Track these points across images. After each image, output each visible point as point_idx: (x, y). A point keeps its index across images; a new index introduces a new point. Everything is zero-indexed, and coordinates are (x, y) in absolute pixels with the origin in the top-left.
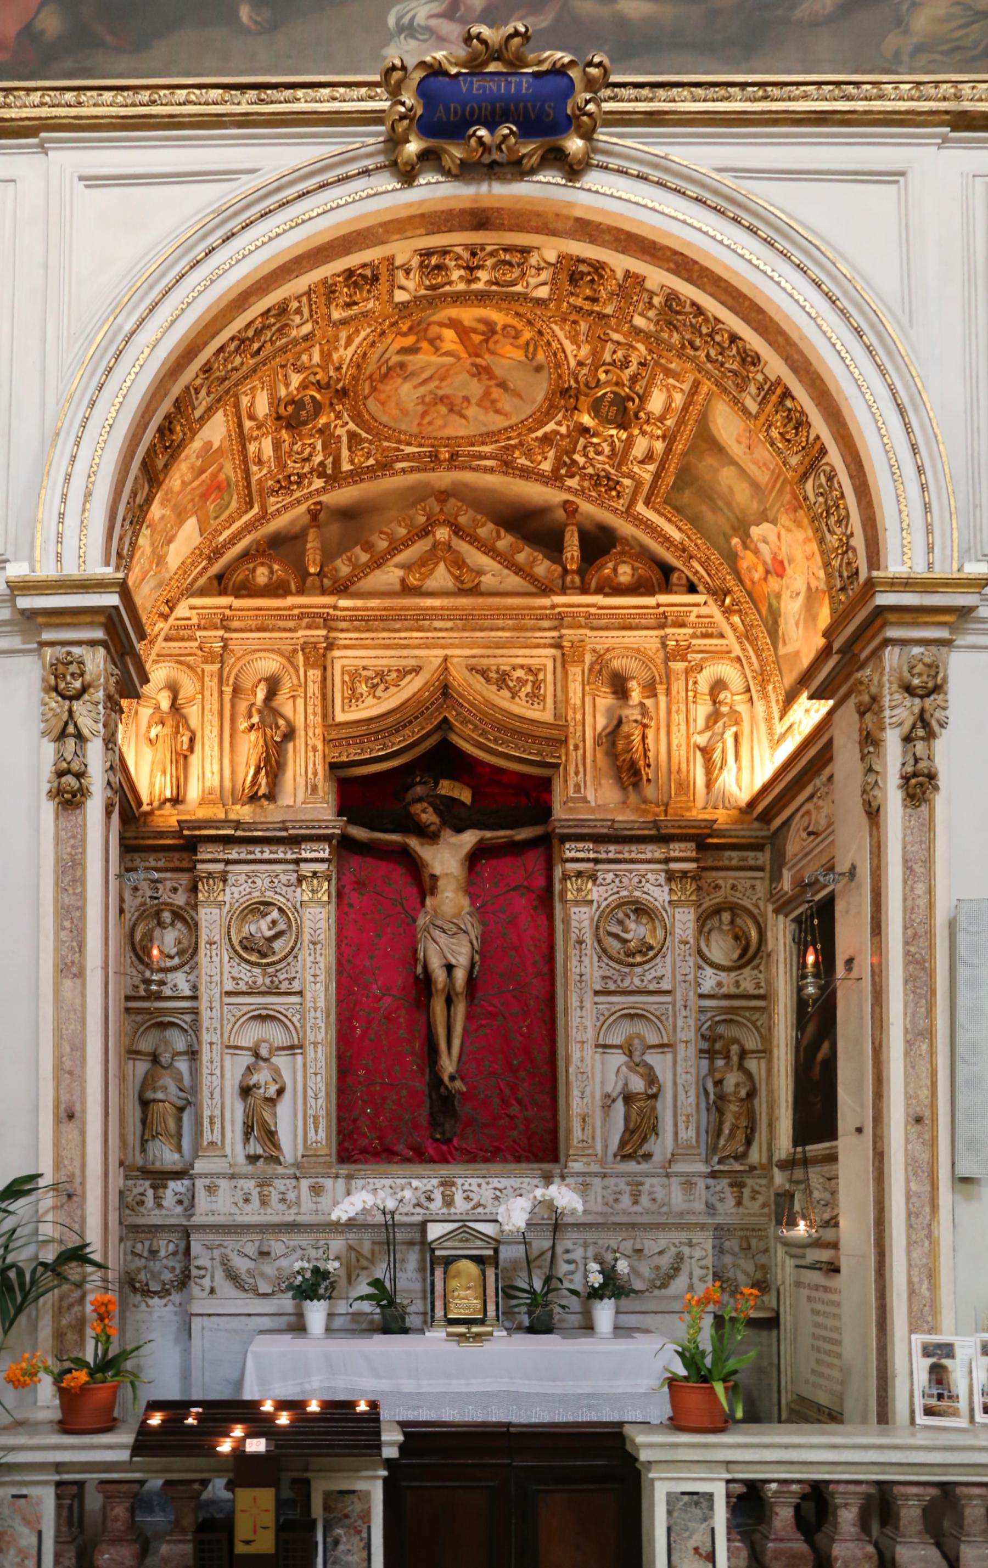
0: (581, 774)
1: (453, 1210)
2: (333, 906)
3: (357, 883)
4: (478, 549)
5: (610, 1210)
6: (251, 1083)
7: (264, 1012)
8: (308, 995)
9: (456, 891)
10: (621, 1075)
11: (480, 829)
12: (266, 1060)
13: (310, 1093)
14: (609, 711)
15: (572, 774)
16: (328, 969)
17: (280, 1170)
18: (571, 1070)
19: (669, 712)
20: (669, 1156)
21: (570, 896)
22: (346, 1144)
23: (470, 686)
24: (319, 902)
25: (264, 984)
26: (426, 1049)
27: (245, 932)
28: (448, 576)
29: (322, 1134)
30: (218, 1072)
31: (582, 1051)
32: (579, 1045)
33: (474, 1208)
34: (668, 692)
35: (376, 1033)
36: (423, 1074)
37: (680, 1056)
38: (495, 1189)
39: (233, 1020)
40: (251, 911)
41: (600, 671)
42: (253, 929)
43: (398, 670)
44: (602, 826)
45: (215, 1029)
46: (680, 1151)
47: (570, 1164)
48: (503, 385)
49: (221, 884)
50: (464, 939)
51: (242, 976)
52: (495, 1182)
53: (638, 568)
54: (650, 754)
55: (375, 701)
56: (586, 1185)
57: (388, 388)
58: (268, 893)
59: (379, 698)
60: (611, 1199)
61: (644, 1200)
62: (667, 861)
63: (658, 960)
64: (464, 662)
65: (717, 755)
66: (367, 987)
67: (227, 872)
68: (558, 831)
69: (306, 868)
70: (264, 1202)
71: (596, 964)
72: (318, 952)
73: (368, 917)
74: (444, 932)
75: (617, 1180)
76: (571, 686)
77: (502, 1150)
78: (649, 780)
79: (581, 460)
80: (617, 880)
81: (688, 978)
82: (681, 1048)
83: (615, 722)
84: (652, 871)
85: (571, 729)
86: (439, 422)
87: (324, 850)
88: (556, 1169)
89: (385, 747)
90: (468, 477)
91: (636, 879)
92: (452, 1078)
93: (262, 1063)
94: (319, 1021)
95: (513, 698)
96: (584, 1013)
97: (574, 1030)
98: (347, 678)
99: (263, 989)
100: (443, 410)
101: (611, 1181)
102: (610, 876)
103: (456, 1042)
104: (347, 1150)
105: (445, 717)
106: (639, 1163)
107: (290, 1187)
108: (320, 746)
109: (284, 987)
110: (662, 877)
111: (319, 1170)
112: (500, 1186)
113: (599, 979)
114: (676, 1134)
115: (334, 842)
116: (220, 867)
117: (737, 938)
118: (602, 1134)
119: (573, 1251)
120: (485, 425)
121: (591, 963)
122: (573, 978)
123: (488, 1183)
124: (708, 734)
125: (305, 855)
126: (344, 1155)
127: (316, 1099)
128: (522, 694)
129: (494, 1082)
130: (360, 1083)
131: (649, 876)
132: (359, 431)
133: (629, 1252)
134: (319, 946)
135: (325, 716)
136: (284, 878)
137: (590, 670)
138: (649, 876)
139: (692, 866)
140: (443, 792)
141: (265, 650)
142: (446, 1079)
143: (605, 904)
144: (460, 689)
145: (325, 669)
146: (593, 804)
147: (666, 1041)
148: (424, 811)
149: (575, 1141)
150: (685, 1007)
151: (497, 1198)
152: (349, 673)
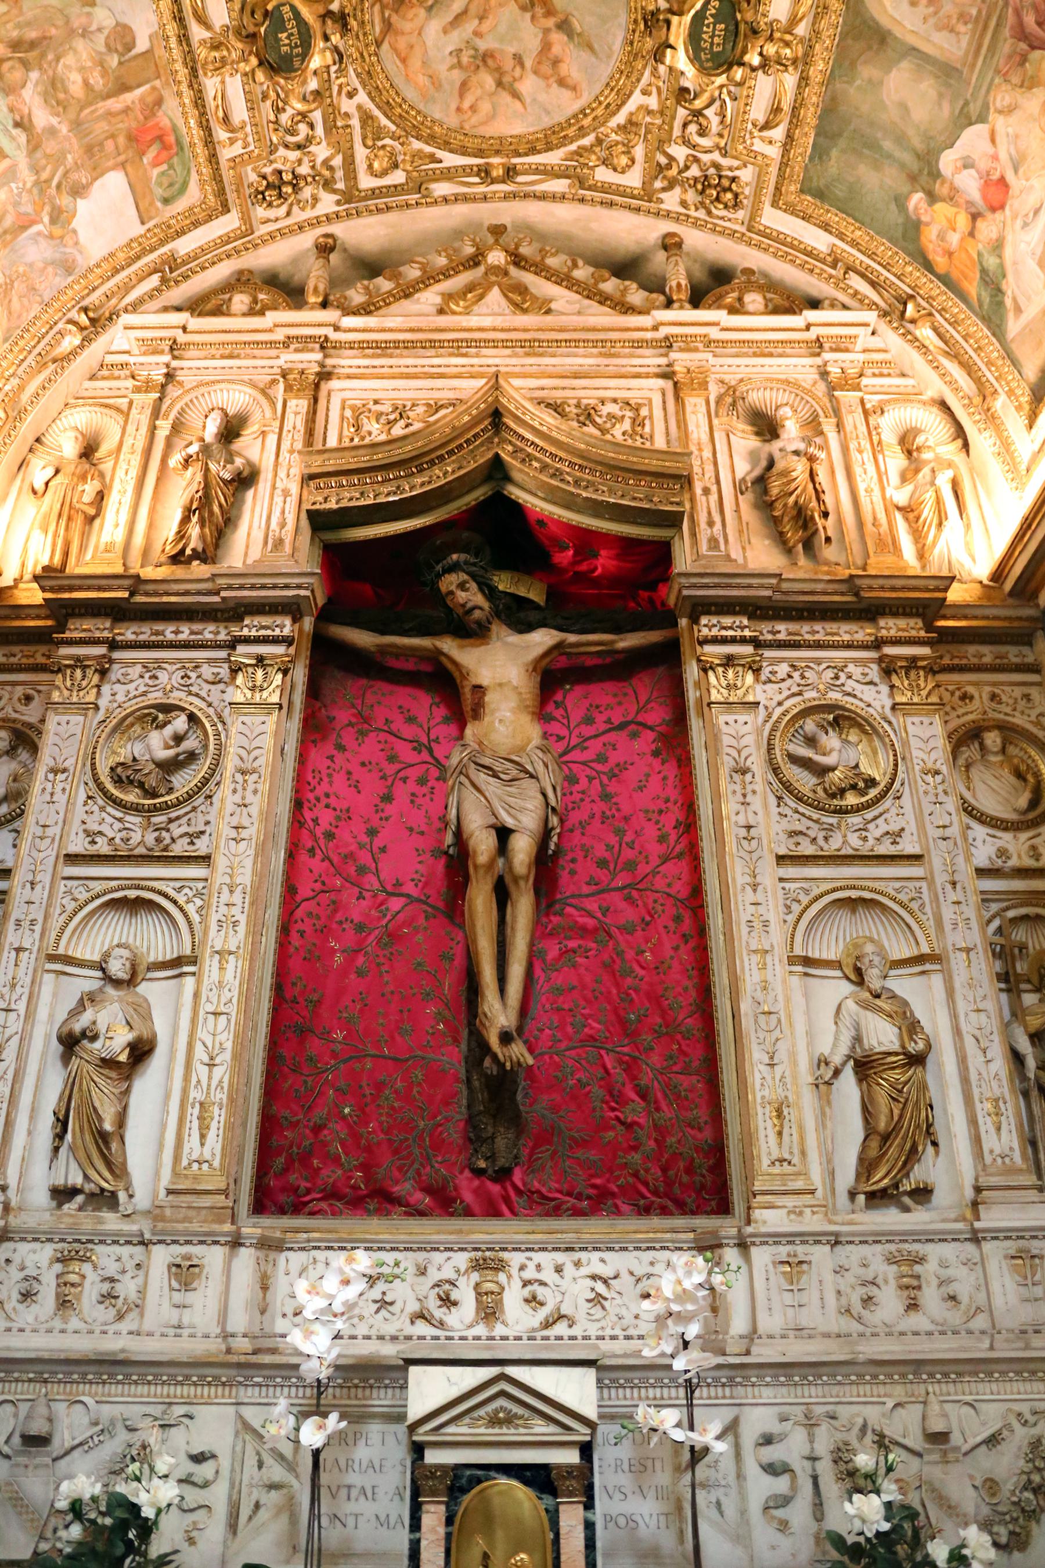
1: (499, 1330)
4: (548, 279)
5: (855, 1327)
6: (77, 1027)
7: (132, 894)
10: (846, 1019)
12: (117, 983)
13: (200, 1053)
14: (753, 456)
16: (267, 816)
17: (111, 1221)
18: (745, 1007)
19: (845, 450)
20: (969, 1193)
21: (715, 696)
24: (266, 707)
25: (142, 842)
27: (124, 754)
28: (504, 302)
29: (214, 1142)
30: (22, 1007)
32: (756, 958)
33: (547, 1325)
34: (839, 426)
37: (959, 981)
38: (594, 1277)
39: (71, 906)
40: (141, 719)
41: (734, 404)
42: (138, 749)
44: (762, 587)
45: (33, 922)
46: (994, 1181)
47: (757, 1214)
48: (564, 26)
49: (96, 679)
51: (105, 828)
52: (594, 1262)
53: (771, 300)
54: (828, 498)
56: (795, 1267)
57: (407, 26)
58: (176, 694)
60: (855, 1300)
61: (931, 1297)
62: (878, 644)
63: (887, 803)
65: (928, 512)
67: (111, 661)
69: (244, 653)
70: (64, 1303)
71: (774, 810)
72: (251, 787)
75: (865, 1250)
78: (828, 540)
79: (680, 152)
80: (796, 675)
81: (948, 833)
82: (958, 962)
83: (764, 463)
84: (855, 661)
86: (485, 107)
88: (727, 1227)
90: (533, 212)
91: (830, 674)
92: (506, 1038)
93: (110, 991)
94: (235, 911)
96: (760, 897)
97: (745, 930)
99: (141, 850)
100: (488, 81)
101: (853, 1254)
102: (783, 669)
103: (516, 972)
106: (906, 1209)
107: (130, 1265)
109: (179, 848)
110: (874, 672)
111: (195, 1227)
112: (606, 1271)
113: (783, 837)
114: (977, 1140)
116: (101, 650)
117: (1020, 776)
118: (822, 1144)
119: (783, 1437)
120: (547, 112)
121: (766, 805)
122: (732, 833)
123: (578, 1264)
124: (909, 488)
127: (211, 1066)
131: (851, 668)
132: (377, 113)
133: (915, 1441)
136: (207, 671)
138: (851, 668)
139: (925, 651)
141: (229, 381)
142: (494, 1041)
143: (779, 711)
147: (925, 949)
148: (462, 586)
149: (765, 1162)
150: (954, 884)
151: (598, 1300)
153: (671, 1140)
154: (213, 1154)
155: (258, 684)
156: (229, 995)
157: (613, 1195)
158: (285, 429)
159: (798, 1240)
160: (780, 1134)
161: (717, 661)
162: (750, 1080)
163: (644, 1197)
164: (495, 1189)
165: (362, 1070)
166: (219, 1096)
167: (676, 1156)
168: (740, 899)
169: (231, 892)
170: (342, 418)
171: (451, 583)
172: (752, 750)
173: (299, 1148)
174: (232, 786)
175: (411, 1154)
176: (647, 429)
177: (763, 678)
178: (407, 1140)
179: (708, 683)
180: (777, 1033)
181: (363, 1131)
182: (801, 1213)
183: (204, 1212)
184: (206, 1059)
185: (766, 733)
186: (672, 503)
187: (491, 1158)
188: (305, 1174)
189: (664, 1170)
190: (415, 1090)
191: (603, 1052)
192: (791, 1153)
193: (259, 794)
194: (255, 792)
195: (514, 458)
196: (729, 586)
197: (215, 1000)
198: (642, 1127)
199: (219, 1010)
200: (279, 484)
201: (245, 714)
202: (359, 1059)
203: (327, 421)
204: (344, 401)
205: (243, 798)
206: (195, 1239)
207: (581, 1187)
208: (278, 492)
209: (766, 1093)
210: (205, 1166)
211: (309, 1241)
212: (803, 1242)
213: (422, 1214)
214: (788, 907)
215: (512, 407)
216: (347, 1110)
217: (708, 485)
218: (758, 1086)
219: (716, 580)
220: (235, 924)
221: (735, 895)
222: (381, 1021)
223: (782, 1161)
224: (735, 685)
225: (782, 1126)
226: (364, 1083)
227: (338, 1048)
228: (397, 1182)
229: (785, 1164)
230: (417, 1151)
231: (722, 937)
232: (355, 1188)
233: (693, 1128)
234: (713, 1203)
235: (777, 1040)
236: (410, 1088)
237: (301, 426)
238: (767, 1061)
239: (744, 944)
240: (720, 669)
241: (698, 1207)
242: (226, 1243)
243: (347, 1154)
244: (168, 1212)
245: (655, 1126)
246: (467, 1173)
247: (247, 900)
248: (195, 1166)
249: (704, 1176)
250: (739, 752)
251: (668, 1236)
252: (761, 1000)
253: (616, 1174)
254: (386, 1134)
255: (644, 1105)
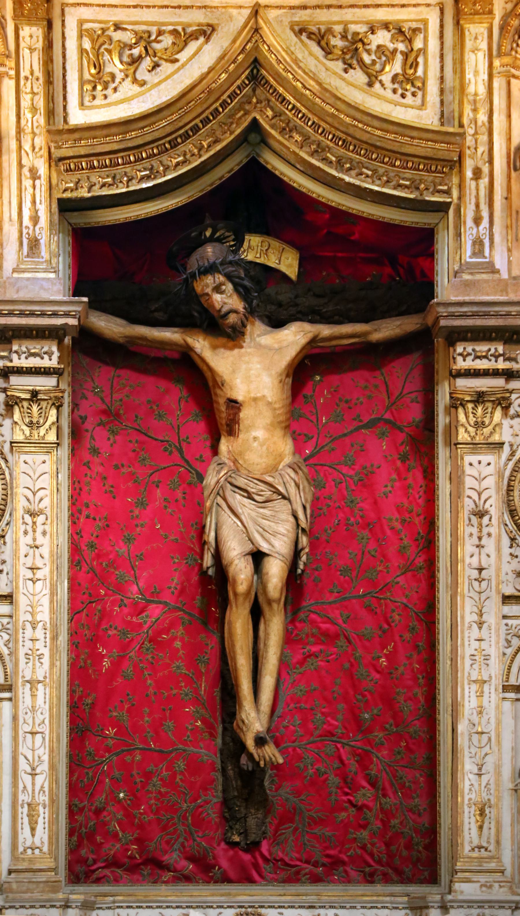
0: (485, 223)
2: (64, 451)
3: (105, 412)
8: (22, 601)
9: (270, 428)
11: (312, 322)
13: (23, 765)
15: (470, 223)
16: (55, 557)
18: (461, 728)
21: (462, 436)
22: (83, 852)
23: (296, 61)
26: (217, 693)
31: (481, 695)
32: (474, 687)
35: (135, 666)
36: (213, 736)
43: (175, 33)
47: (457, 886)
50: (281, 505)
55: (136, 89)
59: (143, 83)
64: (287, 17)
66: (121, 588)
68: (443, 323)
71: (506, 550)
72: (40, 529)
73: (125, 470)
74: (250, 497)
76: (470, 58)
77: (344, 863)
85: (469, 141)
87: (50, 354)
89: (153, 174)
92: (260, 741)
94: (39, 645)
95: (370, 84)
97: (468, 662)
98: (87, 45)
104: (84, 861)
105: (255, 121)
108: (43, 169)
111: (37, 895)
113: (511, 577)
115: (67, 340)
121: (499, 550)
125: (17, 362)
126: (80, 869)
127: (33, 775)
128: (386, 78)
129: (330, 749)
130: (108, 750)
134: (40, 519)
135: (50, 114)
137: (503, 28)
140: (250, 257)
142: (250, 743)
144: (280, 68)
145: (50, 25)
146: (505, 275)
148: (218, 289)
149: (467, 848)
152: (90, 33)
153: (394, 822)
154: (42, 843)
155: (35, 420)
156: (41, 717)
157: (344, 863)
158: (22, 74)
159: (486, 905)
160: (481, 827)
161: (468, 398)
162: (460, 786)
163: (369, 866)
164: (247, 857)
165: (133, 761)
166: (42, 798)
167: (398, 835)
168: (466, 634)
169: (34, 628)
170: (82, 51)
171: (207, 286)
172: (492, 492)
173: (86, 828)
174: (23, 528)
175: (176, 830)
176: (420, 72)
177: (512, 411)
178: (173, 819)
179: (458, 421)
180: (487, 749)
181: (135, 812)
182: (491, 887)
183: (42, 885)
184: (29, 770)
185: (507, 473)
186: (439, 191)
187: (245, 833)
188: (92, 848)
189: (388, 845)
190: (179, 777)
191: (339, 746)
192: (488, 842)
193: (48, 536)
194: (44, 533)
195: (273, 126)
196: (486, 315)
197: (30, 721)
198: (370, 809)
199: (34, 730)
200: (24, 161)
201: (26, 453)
202: (130, 753)
203: (64, 57)
204: (81, 22)
205: (34, 540)
206: (37, 905)
207: (318, 856)
208: (26, 171)
209: (473, 796)
210: (37, 851)
211: (114, 902)
212: (490, 907)
213: (187, 879)
214: (508, 641)
215: (272, 59)
216: (122, 795)
217: (480, 164)
218: (466, 791)
219: (475, 309)
220: (40, 656)
221: (463, 632)
222: (147, 719)
223: (480, 847)
224: (483, 423)
225: (483, 822)
226: (135, 772)
227: (110, 743)
228: (166, 852)
229: (483, 850)
230: (181, 828)
231: (449, 662)
232: (132, 857)
233: (414, 813)
234: (426, 873)
235: (486, 754)
236: (173, 776)
237: (39, 73)
238: (476, 771)
239: (466, 674)
240: (470, 406)
241: (413, 875)
242: (61, 906)
243: (123, 831)
244: (14, 886)
245: (382, 809)
246: (223, 845)
247: (48, 636)
248: (29, 851)
249: (420, 852)
250: (480, 494)
251: (388, 899)
252: (476, 722)
253: (347, 846)
254: (155, 814)
255: (373, 791)
